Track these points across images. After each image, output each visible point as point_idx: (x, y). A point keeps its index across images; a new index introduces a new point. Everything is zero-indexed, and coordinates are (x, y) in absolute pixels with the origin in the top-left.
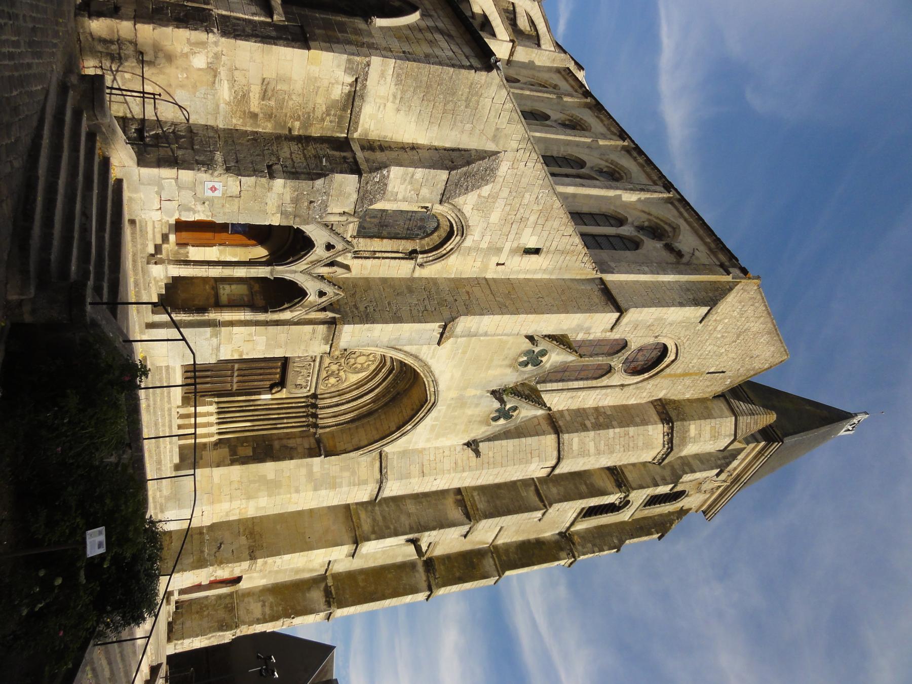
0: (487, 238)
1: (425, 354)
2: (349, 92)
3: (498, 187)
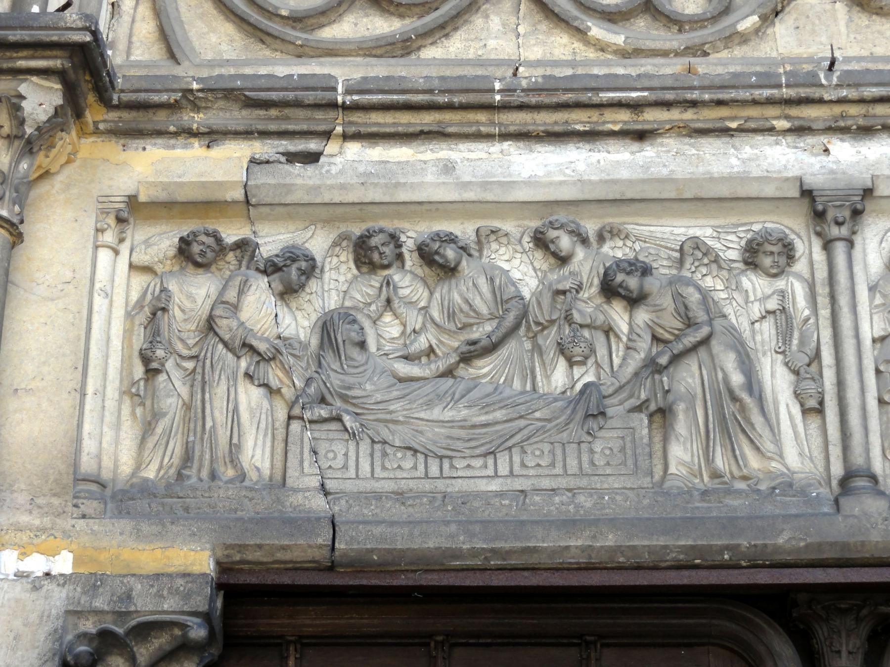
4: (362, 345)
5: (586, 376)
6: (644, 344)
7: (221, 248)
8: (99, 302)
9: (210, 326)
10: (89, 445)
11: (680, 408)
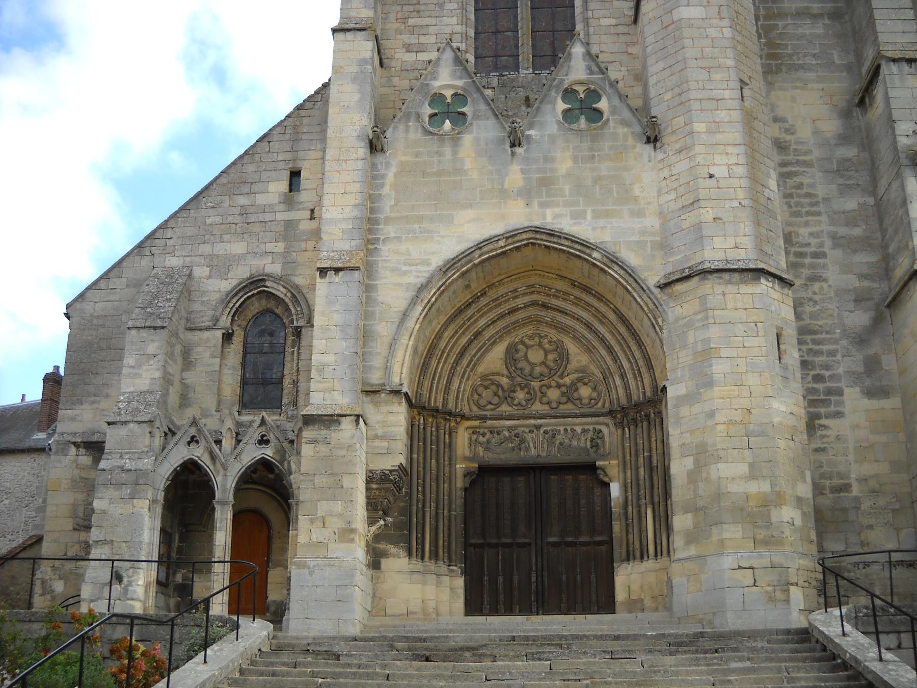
0: (270, 247)
1: (418, 277)
2: (85, 448)
3: (197, 259)
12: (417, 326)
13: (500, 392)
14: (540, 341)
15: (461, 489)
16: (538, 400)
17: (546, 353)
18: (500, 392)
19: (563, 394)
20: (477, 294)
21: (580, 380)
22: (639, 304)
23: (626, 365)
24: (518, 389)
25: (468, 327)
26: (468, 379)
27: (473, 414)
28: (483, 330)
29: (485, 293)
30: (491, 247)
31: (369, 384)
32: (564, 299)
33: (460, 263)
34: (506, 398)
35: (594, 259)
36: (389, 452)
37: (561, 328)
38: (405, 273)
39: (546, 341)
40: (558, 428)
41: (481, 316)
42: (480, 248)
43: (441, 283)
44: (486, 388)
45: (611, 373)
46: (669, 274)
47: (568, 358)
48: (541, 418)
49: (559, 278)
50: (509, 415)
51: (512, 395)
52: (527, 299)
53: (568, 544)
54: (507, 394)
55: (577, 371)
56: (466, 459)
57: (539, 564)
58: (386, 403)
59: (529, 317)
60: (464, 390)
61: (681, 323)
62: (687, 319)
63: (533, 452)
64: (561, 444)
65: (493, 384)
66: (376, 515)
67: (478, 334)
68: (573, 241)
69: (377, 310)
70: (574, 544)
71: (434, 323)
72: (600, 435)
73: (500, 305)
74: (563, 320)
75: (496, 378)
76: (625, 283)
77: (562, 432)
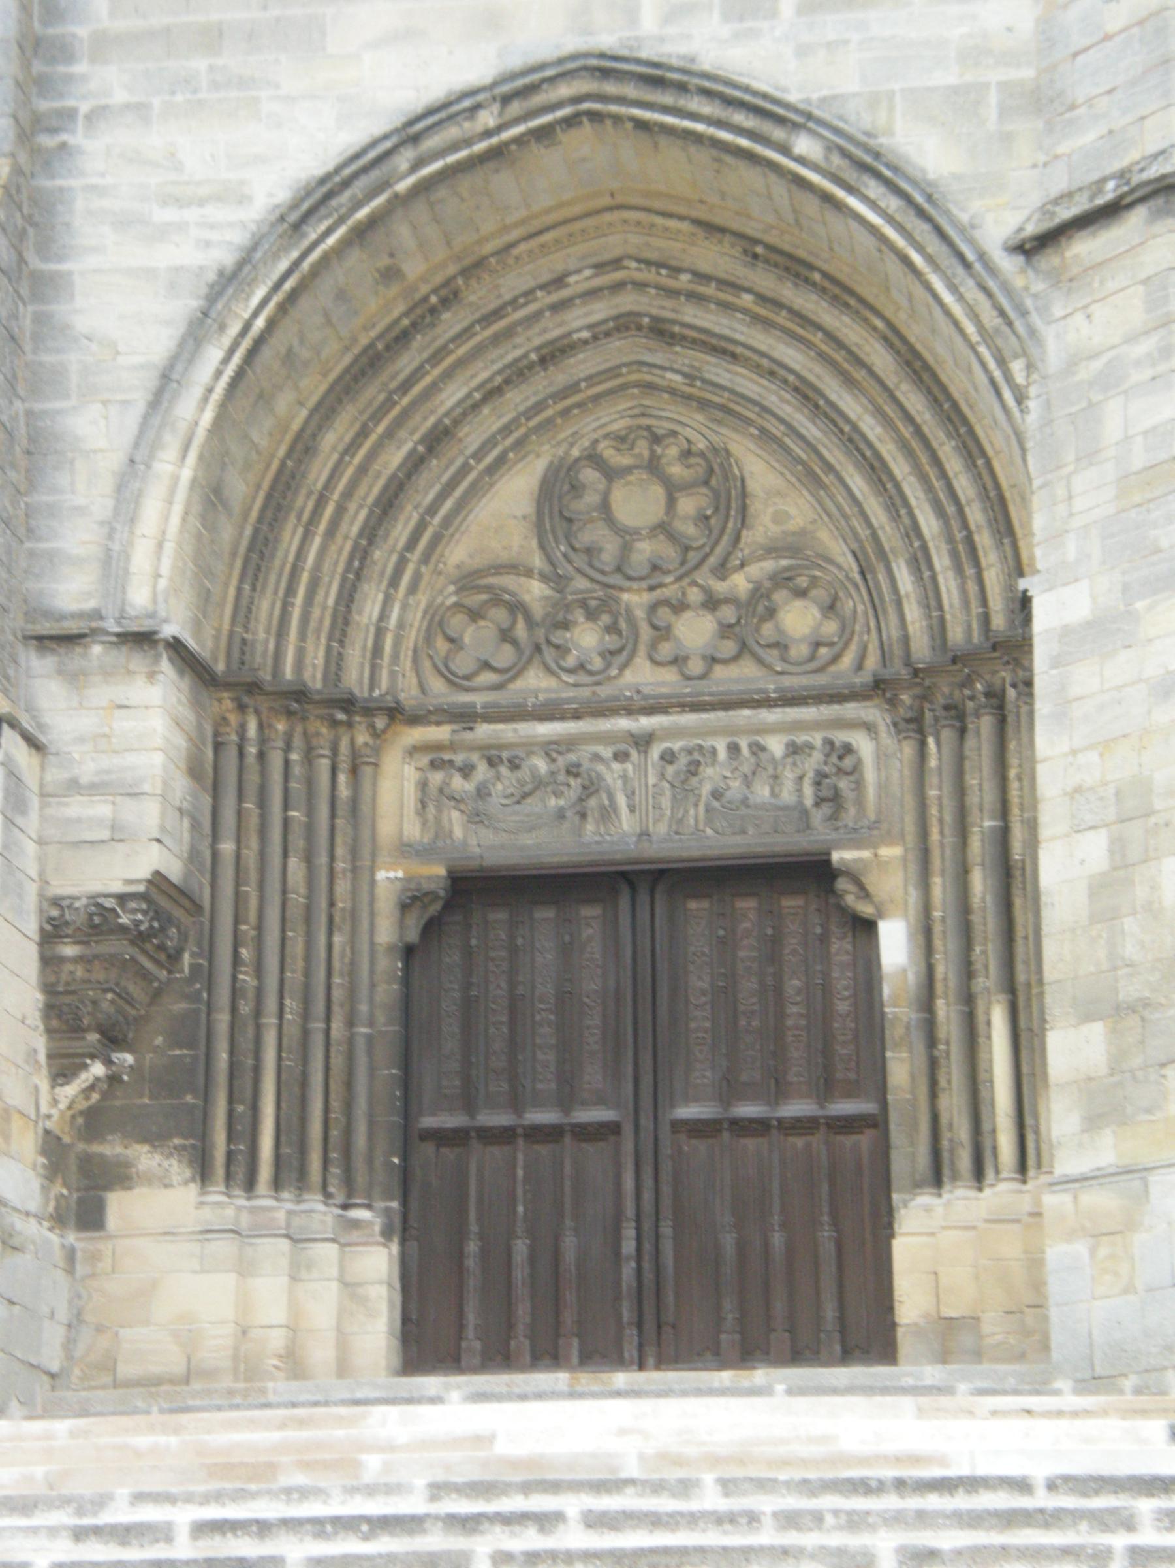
1: (208, 244)
4: (489, 795)
5: (562, 802)
6: (580, 789)
7: (443, 761)
8: (406, 783)
9: (441, 791)
10: (406, 833)
11: (589, 813)
12: (208, 417)
13: (521, 630)
14: (653, 452)
15: (391, 948)
16: (642, 650)
17: (672, 491)
18: (521, 630)
19: (726, 630)
20: (425, 299)
21: (782, 580)
22: (947, 313)
23: (929, 524)
24: (579, 615)
25: (405, 415)
26: (413, 589)
27: (431, 702)
28: (456, 423)
29: (456, 294)
30: (452, 132)
31: (48, 614)
32: (725, 306)
33: (347, 194)
34: (538, 649)
35: (801, 160)
36: (118, 835)
37: (723, 408)
38: (162, 233)
39: (673, 451)
40: (708, 743)
41: (448, 375)
42: (415, 139)
43: (283, 265)
44: (475, 615)
45: (882, 554)
46: (1056, 201)
47: (744, 509)
48: (650, 711)
49: (700, 233)
50: (547, 704)
51: (558, 637)
52: (600, 310)
53: (742, 1127)
54: (540, 633)
55: (772, 550)
56: (406, 850)
57: (647, 1196)
58: (108, 673)
59: (613, 372)
60: (401, 625)
61: (1084, 373)
62: (1104, 359)
63: (627, 823)
64: (716, 794)
65: (497, 601)
66: (77, 1047)
67: (438, 438)
68: (729, 102)
69: (73, 360)
70: (759, 1127)
71: (283, 402)
72: (848, 763)
73: (509, 333)
74: (724, 378)
75: (508, 581)
76: (900, 242)
77: (722, 754)
